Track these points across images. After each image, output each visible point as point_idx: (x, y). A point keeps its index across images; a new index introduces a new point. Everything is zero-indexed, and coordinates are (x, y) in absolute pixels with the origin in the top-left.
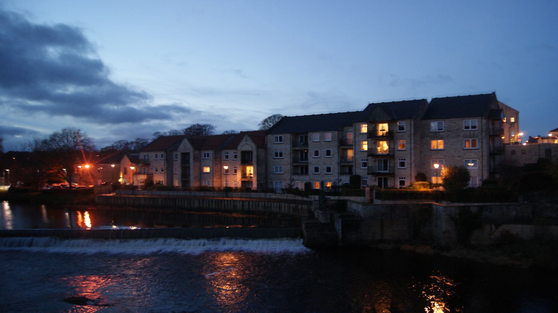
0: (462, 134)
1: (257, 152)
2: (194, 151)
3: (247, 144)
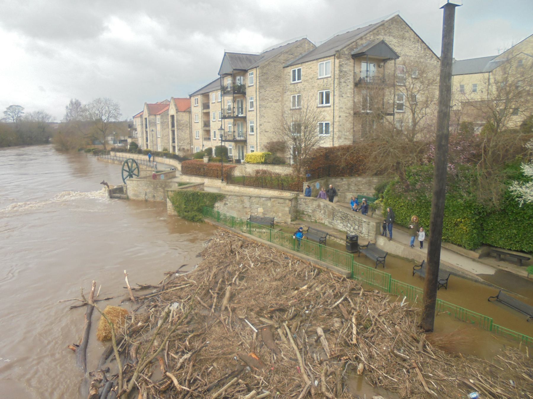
0: (316, 85)
1: (177, 116)
2: (149, 116)
3: (172, 108)
